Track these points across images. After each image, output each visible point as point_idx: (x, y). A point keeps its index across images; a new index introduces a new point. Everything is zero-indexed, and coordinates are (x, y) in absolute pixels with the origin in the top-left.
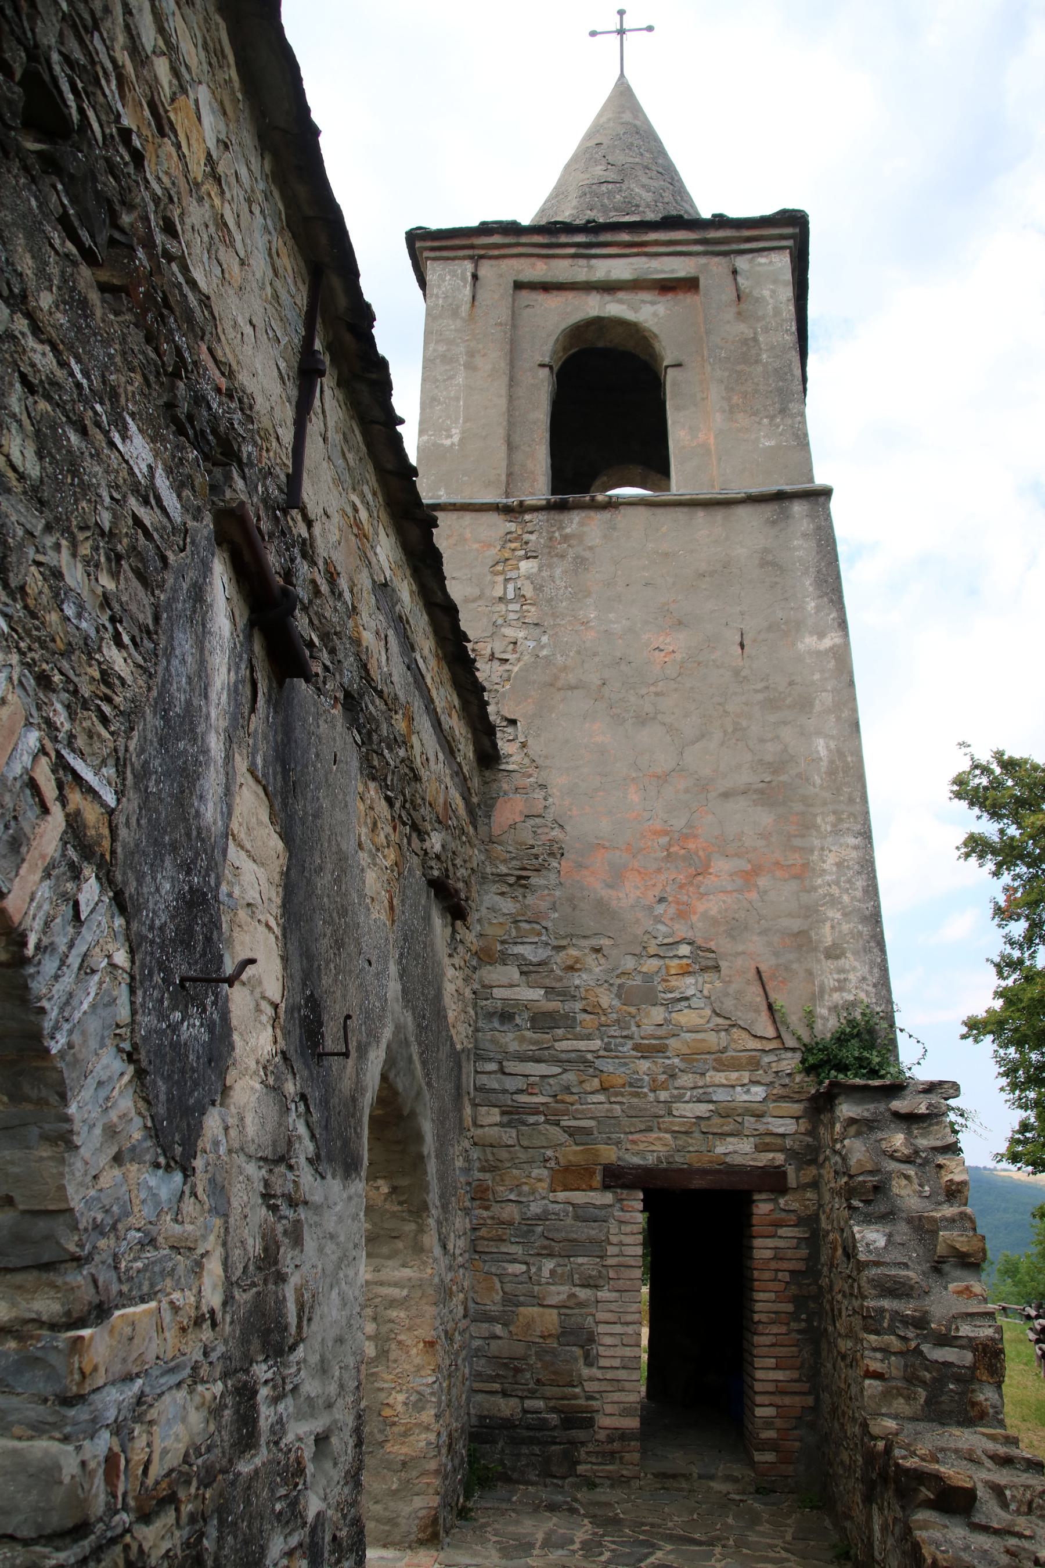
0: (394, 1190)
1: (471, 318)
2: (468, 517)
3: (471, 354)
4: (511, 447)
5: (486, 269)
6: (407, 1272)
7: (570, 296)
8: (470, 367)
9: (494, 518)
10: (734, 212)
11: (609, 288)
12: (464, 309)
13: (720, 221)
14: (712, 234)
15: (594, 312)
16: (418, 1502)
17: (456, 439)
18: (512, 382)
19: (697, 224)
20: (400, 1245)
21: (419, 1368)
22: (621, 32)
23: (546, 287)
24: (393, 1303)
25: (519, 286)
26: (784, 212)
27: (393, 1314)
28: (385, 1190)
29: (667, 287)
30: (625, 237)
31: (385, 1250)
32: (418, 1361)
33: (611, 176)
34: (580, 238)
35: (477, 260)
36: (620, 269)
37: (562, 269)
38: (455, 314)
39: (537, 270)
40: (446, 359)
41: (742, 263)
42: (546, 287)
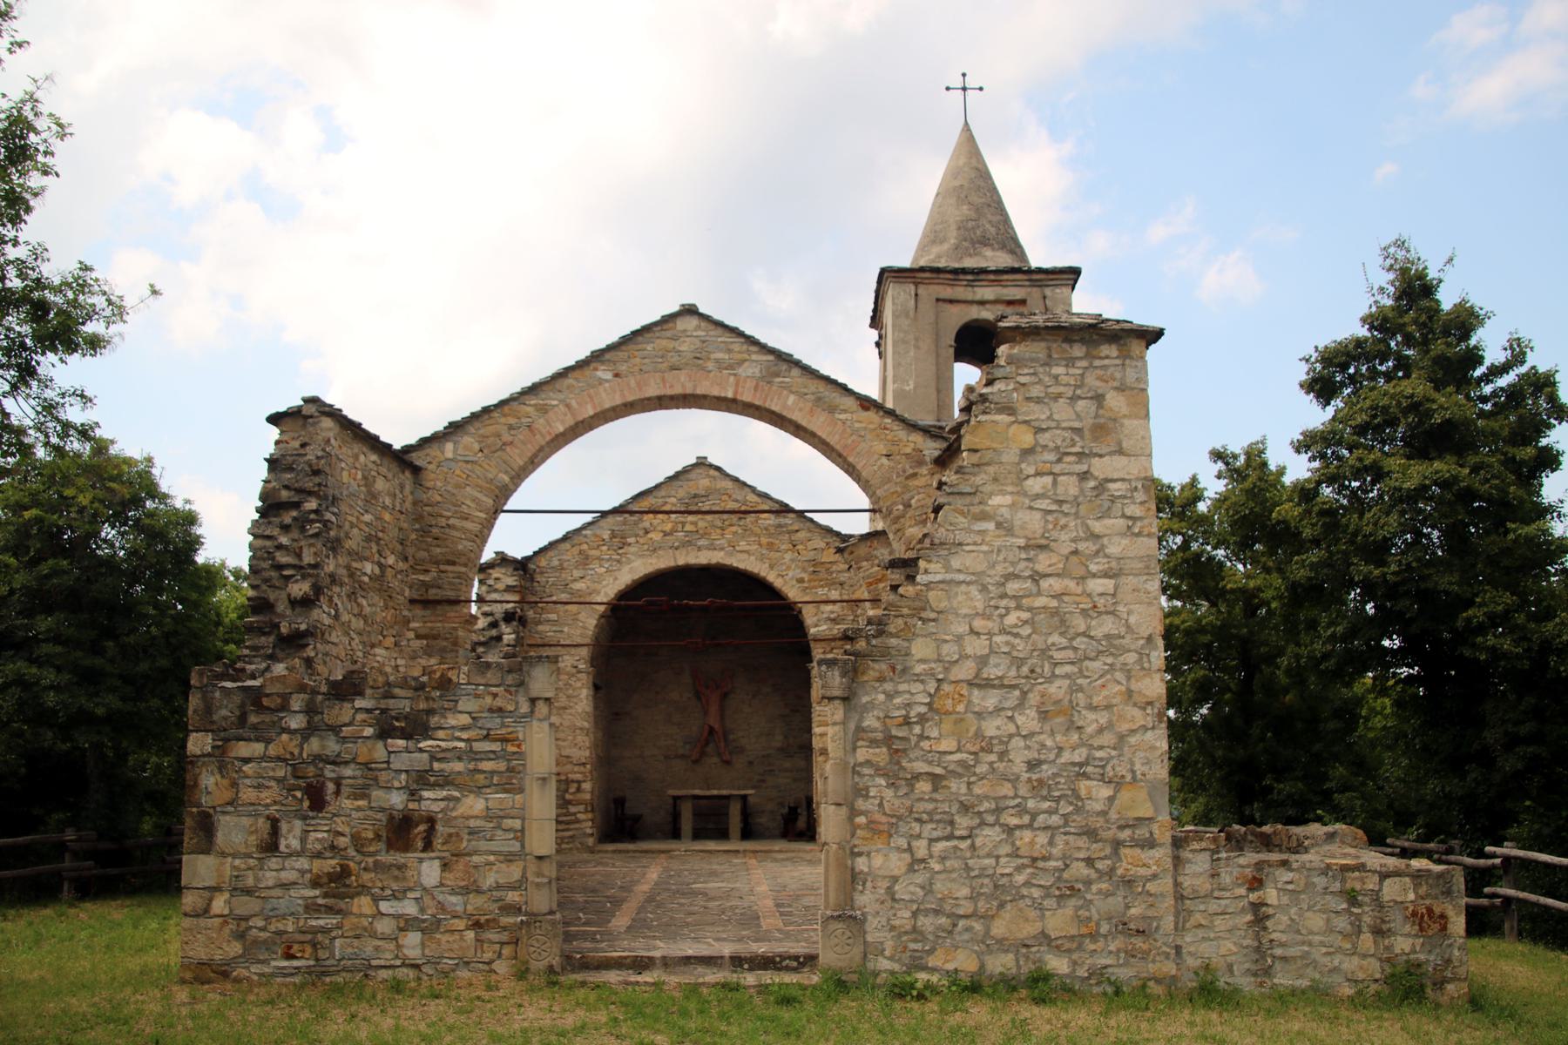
1: (915, 319)
3: (917, 339)
4: (938, 391)
5: (922, 290)
7: (963, 306)
8: (917, 347)
10: (1045, 266)
11: (982, 303)
12: (912, 313)
13: (1040, 271)
14: (1035, 277)
15: (975, 316)
18: (938, 355)
19: (1030, 271)
22: (964, 89)
23: (951, 301)
25: (938, 300)
29: (1010, 303)
30: (992, 277)
33: (974, 216)
34: (970, 277)
35: (916, 284)
36: (988, 293)
37: (960, 292)
38: (907, 316)
39: (947, 292)
40: (904, 342)
41: (1048, 291)
42: (951, 301)
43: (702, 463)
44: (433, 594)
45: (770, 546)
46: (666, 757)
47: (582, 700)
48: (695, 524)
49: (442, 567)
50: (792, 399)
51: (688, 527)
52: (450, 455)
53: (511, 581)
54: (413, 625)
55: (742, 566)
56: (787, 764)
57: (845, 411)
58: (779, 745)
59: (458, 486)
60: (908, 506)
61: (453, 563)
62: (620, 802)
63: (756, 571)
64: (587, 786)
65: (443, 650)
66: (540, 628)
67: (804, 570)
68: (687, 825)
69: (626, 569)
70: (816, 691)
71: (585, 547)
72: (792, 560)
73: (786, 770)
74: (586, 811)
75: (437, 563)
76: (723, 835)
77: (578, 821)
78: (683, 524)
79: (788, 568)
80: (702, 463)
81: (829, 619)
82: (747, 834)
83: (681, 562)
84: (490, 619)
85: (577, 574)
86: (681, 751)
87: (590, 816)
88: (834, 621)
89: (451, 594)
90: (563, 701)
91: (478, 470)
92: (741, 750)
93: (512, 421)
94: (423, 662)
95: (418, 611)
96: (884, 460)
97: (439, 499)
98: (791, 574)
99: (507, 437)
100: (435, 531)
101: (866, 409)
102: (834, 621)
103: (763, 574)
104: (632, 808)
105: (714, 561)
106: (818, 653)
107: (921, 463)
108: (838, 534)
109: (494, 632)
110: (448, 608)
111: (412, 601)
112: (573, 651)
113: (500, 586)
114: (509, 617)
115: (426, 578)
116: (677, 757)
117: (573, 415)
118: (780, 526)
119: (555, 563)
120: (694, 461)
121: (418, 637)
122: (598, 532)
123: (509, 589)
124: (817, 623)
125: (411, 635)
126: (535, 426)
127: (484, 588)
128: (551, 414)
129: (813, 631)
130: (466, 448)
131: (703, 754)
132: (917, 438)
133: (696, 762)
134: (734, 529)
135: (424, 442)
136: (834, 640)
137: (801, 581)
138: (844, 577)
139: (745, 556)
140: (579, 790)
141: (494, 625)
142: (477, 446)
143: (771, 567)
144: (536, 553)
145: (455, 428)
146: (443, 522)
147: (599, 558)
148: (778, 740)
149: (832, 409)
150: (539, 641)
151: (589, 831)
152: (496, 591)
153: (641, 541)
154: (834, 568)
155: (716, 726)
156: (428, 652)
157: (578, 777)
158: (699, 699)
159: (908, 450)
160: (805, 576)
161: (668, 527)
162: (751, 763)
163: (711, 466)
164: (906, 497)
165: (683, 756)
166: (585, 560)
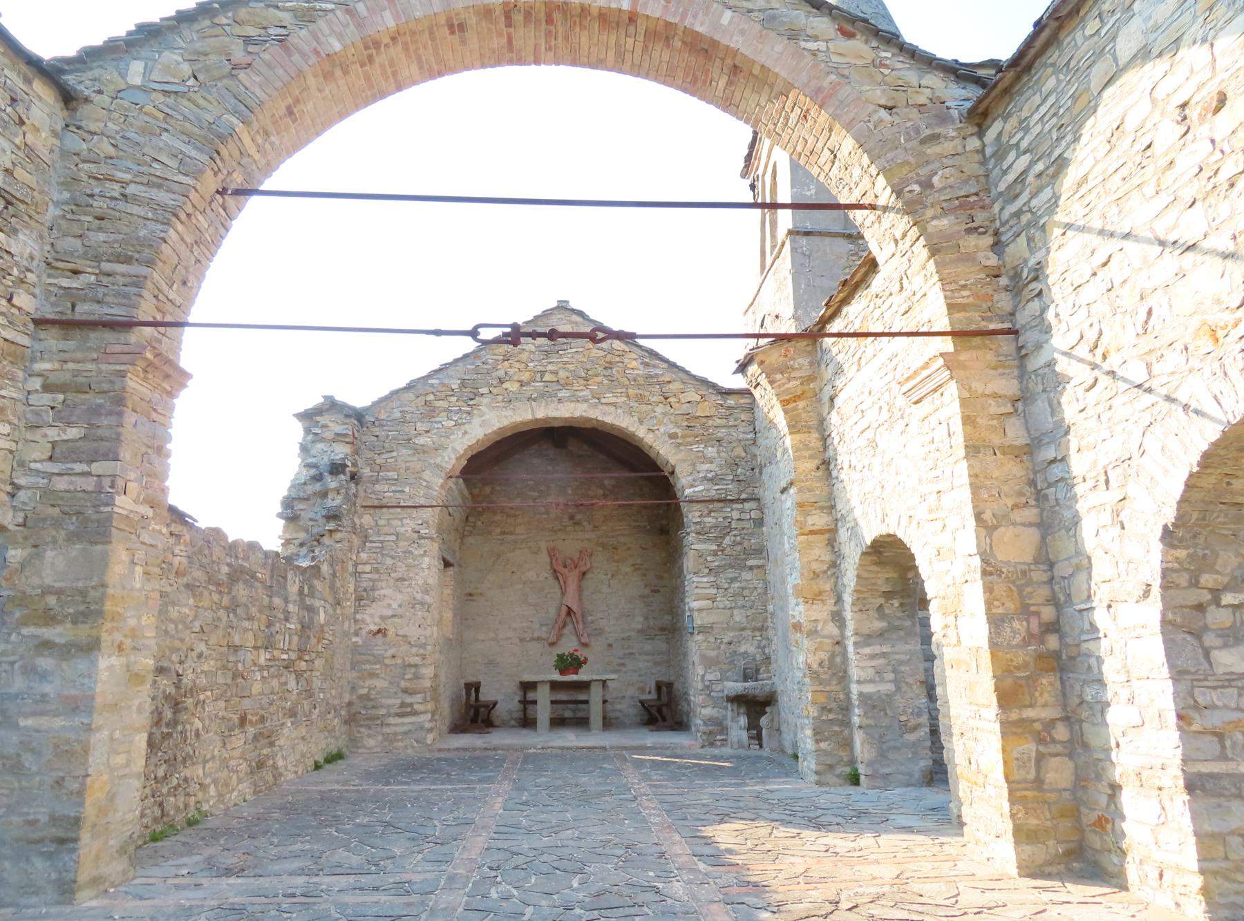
0: (901, 605)
2: (827, 240)
6: (908, 647)
9: (840, 240)
16: (922, 764)
17: (813, 192)
20: (902, 633)
21: (918, 695)
24: (901, 663)
26: (992, 61)
27: (903, 668)
28: (897, 605)
31: (894, 636)
32: (917, 691)
43: (563, 307)
44: (84, 310)
45: (640, 399)
46: (522, 640)
47: (426, 567)
48: (555, 373)
49: (106, 266)
50: (728, 14)
51: (547, 377)
52: (137, 80)
53: (339, 429)
54: (40, 366)
55: (608, 420)
56: (648, 647)
57: (815, 38)
58: (639, 626)
59: (146, 131)
60: (927, 185)
61: (128, 260)
62: (473, 687)
63: (623, 425)
64: (428, 672)
65: (95, 411)
66: (377, 487)
67: (677, 425)
68: (543, 712)
69: (476, 421)
70: (689, 562)
71: (431, 397)
72: (664, 414)
73: (647, 654)
74: (425, 701)
75: (97, 259)
76: (582, 723)
77: (415, 713)
78: (543, 373)
79: (661, 423)
80: (563, 307)
81: (705, 478)
82: (608, 723)
83: (540, 415)
84: (313, 472)
85: (421, 427)
86: (536, 635)
87: (430, 706)
88: (711, 480)
89: (116, 312)
90: (401, 570)
91: (186, 107)
92: (600, 632)
93: (251, 31)
94: (53, 434)
95: (52, 340)
96: (883, 113)
97: (111, 151)
98: (662, 430)
99: (239, 55)
100: (99, 203)
101: (849, 35)
102: (711, 480)
103: (632, 429)
104: (486, 695)
105: (577, 414)
106: (692, 515)
107: (943, 119)
108: (714, 386)
109: (318, 487)
110: (108, 336)
111: (39, 323)
112: (414, 512)
113: (328, 435)
114: (336, 469)
115: (74, 283)
116: (532, 639)
117: (360, 25)
118: (650, 376)
119: (397, 415)
120: (555, 305)
121: (47, 388)
122: (446, 381)
123: (338, 438)
124: (689, 484)
125: (36, 383)
126: (293, 40)
127: (310, 437)
128: (321, 23)
129: (687, 492)
130: (166, 69)
131: (560, 636)
132: (934, 81)
133: (552, 644)
134: (599, 379)
135: (89, 56)
136: (712, 501)
137: (673, 436)
138: (721, 433)
139: (612, 409)
140: (417, 677)
141: (318, 478)
142: (186, 69)
143: (641, 422)
144: (375, 404)
145: (148, 35)
146: (116, 190)
147: (447, 410)
148: (638, 623)
149: (793, 35)
150: (376, 503)
151: (428, 725)
152: (322, 440)
153: (495, 391)
154: (710, 423)
155: (574, 608)
156: (63, 416)
157: (417, 660)
158: (557, 578)
159: (922, 100)
160: (679, 431)
161: (525, 376)
162: (610, 646)
163: (573, 310)
164: (924, 171)
165: (539, 639)
166: (430, 412)
